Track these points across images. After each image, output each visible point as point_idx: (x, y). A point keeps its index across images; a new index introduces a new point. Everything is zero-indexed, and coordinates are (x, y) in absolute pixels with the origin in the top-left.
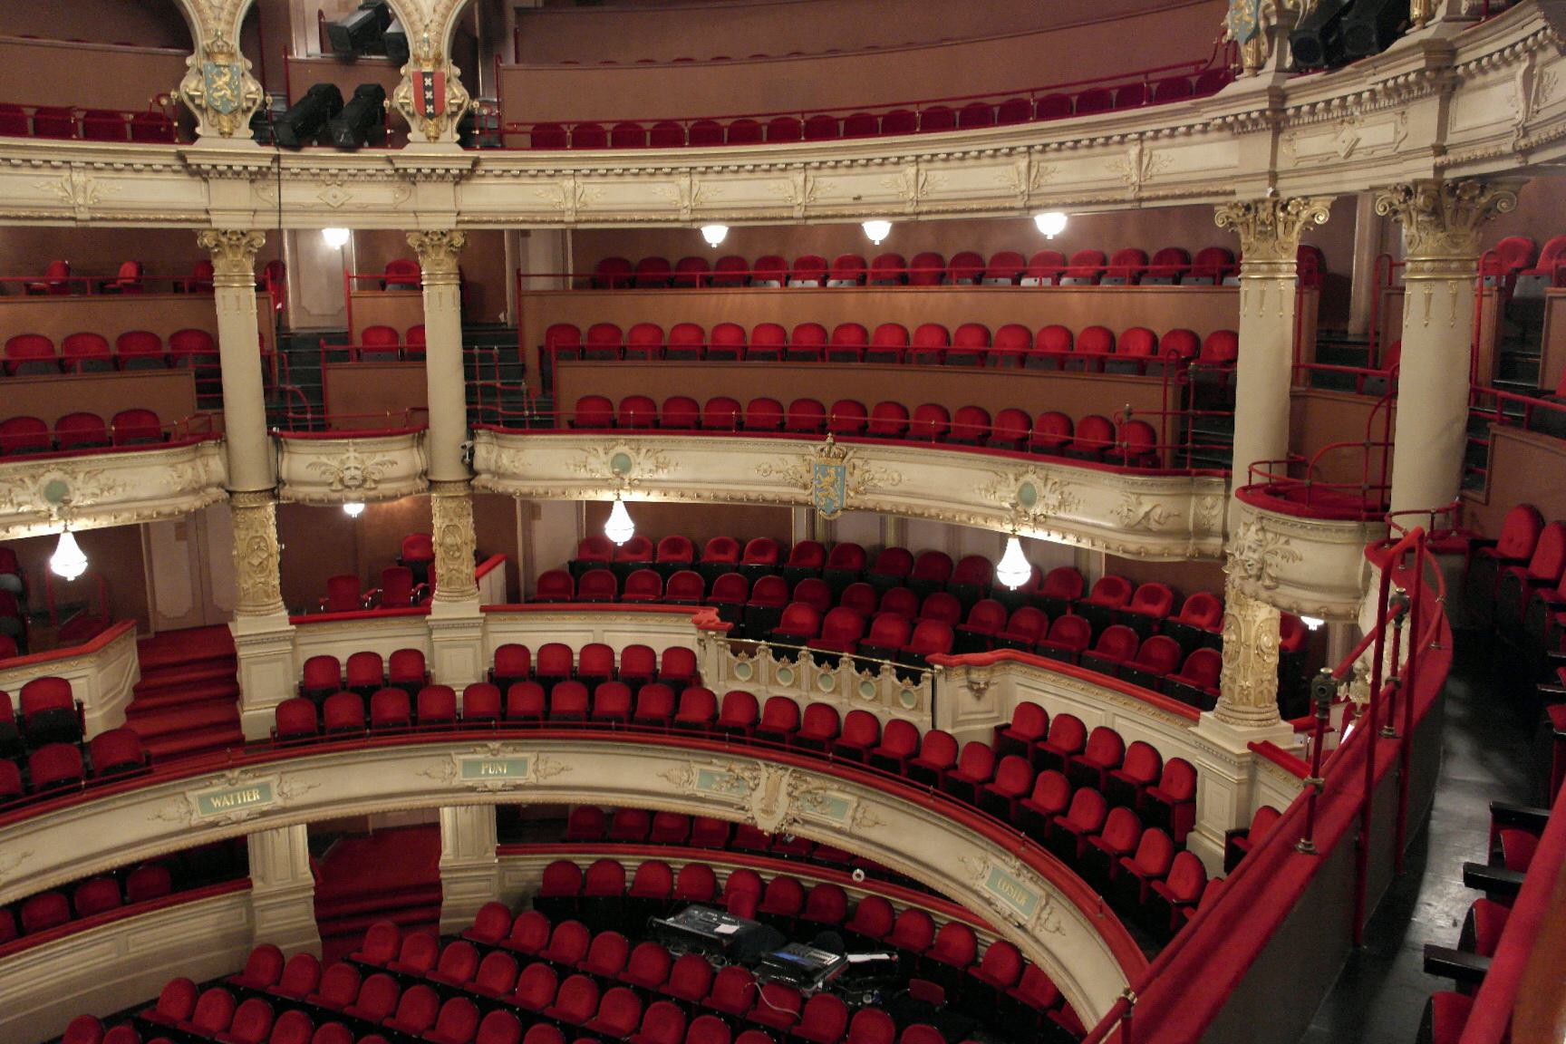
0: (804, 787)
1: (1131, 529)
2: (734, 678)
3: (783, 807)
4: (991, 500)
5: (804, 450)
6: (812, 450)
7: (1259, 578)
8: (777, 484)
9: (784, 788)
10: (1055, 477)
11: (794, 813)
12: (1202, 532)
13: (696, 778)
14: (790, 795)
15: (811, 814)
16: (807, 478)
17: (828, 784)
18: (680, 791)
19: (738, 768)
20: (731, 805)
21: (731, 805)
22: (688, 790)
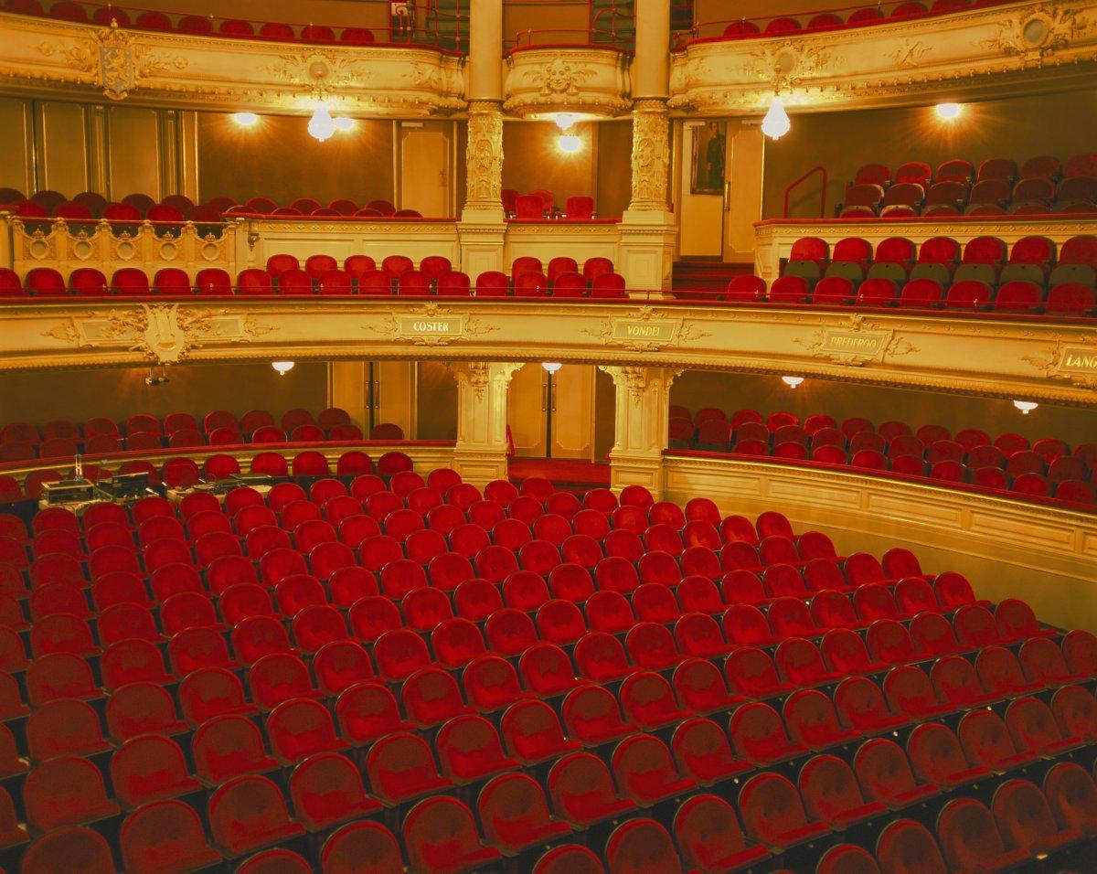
0: (190, 320)
1: (420, 87)
2: (30, 257)
3: (181, 340)
4: (280, 78)
5: (82, 34)
6: (92, 32)
7: (562, 92)
8: (55, 65)
9: (175, 324)
10: (340, 57)
11: (191, 340)
12: (448, 94)
13: (81, 331)
14: (181, 327)
15: (204, 337)
16: (92, 60)
17: (213, 312)
18: (73, 345)
19: (122, 315)
20: (126, 349)
21: (126, 349)
22: (82, 343)
